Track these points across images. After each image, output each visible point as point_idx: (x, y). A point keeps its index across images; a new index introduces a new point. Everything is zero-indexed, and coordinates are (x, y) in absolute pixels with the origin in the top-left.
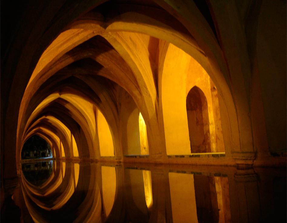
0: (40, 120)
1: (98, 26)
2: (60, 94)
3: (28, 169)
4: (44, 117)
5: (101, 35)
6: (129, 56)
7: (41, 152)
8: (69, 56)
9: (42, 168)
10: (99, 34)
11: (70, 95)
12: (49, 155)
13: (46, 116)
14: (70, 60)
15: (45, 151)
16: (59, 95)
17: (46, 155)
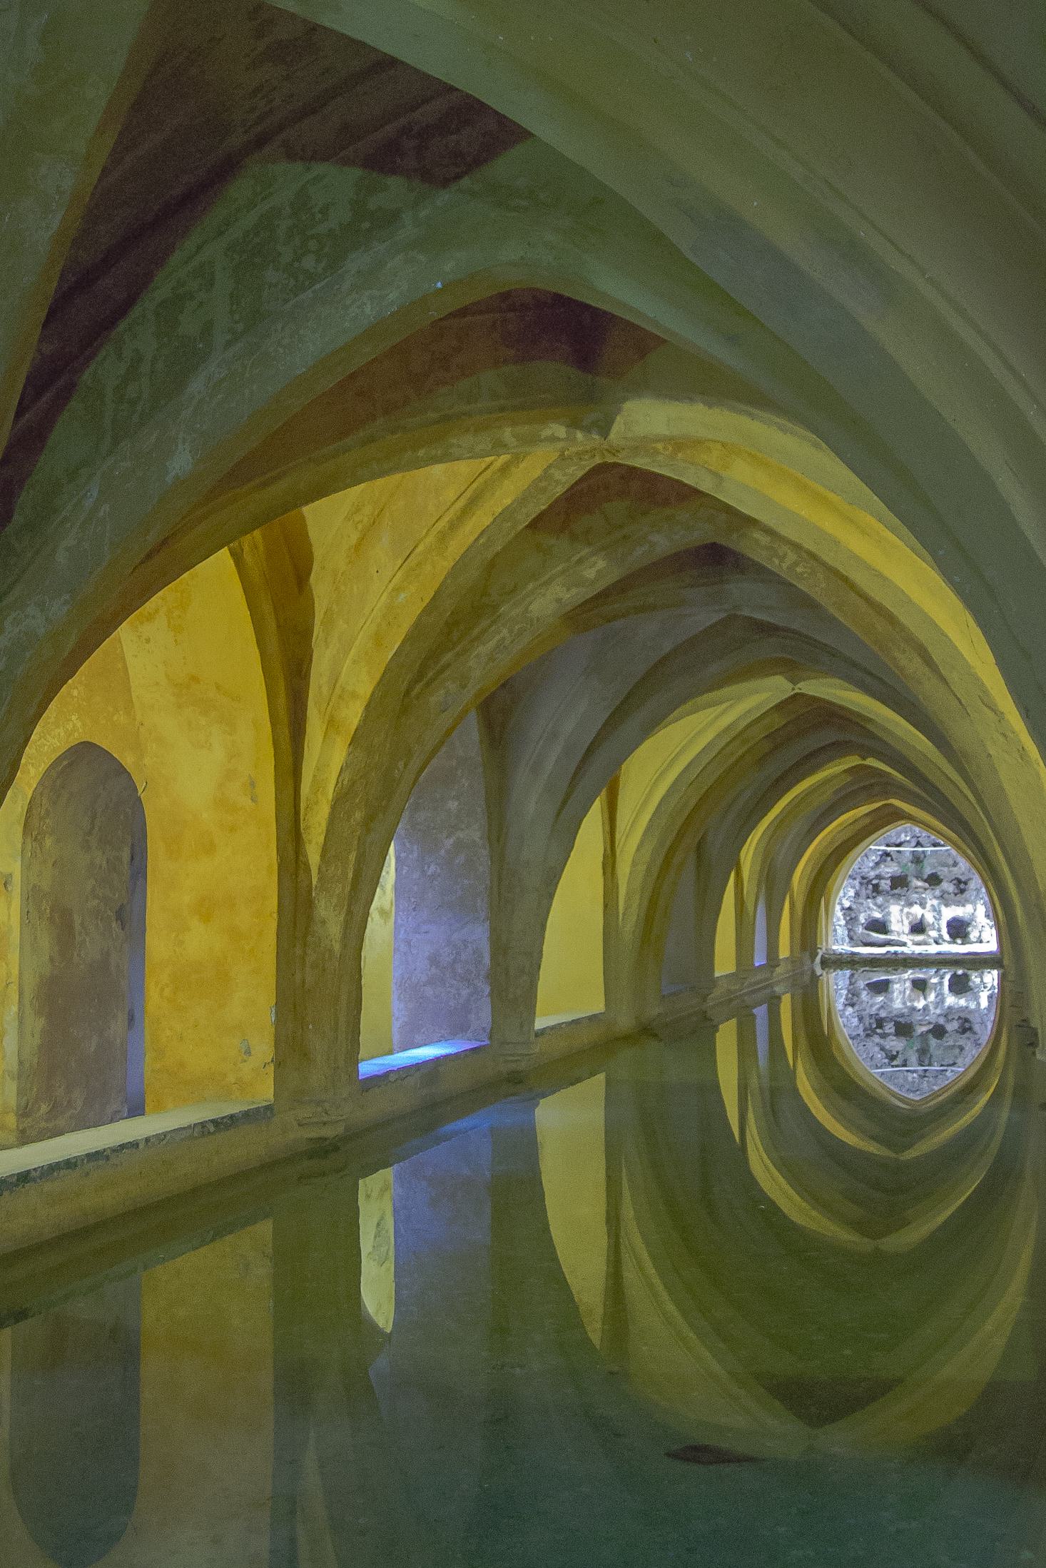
0: (849, 771)
1: (561, 431)
2: (794, 681)
3: (880, 999)
4: (853, 761)
5: (611, 460)
6: (837, 543)
7: (949, 913)
8: (586, 551)
9: (951, 1000)
10: (598, 460)
11: (838, 681)
12: (985, 937)
13: (864, 758)
14: (597, 570)
15: (969, 908)
16: (789, 686)
17: (974, 935)
